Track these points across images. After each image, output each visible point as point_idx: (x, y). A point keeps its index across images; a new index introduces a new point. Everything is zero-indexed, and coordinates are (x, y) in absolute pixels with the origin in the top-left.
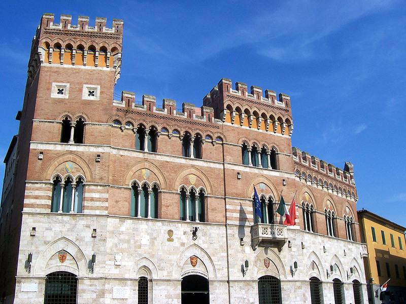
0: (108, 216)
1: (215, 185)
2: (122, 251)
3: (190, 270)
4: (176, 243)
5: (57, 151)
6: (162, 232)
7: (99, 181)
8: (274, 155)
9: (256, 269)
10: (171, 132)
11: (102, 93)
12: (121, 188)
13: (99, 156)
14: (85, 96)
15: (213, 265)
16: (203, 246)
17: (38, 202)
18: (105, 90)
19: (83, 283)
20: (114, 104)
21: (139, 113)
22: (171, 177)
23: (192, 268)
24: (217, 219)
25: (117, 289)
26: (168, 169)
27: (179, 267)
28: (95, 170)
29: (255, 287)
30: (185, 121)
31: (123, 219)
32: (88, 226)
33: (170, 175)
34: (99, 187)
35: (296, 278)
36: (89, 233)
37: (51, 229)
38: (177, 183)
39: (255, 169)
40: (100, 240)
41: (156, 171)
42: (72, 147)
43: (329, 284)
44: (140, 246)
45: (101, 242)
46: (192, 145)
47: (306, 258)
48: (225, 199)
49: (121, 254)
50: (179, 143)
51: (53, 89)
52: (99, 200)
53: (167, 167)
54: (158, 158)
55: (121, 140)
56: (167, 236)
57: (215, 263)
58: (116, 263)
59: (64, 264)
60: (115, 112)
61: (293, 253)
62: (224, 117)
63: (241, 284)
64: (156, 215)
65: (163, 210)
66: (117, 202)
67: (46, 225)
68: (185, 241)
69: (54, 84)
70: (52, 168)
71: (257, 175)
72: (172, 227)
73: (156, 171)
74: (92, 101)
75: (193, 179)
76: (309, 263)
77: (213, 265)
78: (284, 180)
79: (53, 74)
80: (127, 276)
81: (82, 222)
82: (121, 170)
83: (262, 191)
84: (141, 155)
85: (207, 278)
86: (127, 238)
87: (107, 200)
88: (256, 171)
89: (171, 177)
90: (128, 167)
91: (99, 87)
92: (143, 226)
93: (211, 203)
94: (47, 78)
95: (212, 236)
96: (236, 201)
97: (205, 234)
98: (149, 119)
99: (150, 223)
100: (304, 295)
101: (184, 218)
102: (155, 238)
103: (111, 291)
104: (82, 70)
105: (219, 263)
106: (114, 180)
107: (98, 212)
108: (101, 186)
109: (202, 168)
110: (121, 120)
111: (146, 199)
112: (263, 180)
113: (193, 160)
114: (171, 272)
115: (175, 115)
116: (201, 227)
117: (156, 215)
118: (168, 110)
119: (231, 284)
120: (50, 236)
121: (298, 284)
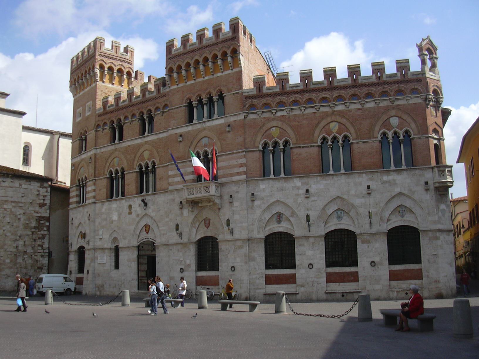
0: (95, 203)
4: (134, 215)
9: (194, 230)
16: (153, 214)
29: (192, 250)
31: (103, 203)
35: (236, 235)
38: (136, 162)
39: (191, 126)
43: (311, 240)
47: (258, 212)
50: (137, 124)
56: (128, 210)
61: (234, 209)
63: (179, 247)
64: (123, 195)
66: (100, 190)
68: (139, 212)
71: (200, 131)
75: (146, 154)
76: (268, 216)
80: (105, 246)
83: (205, 145)
84: (113, 147)
88: (199, 126)
92: (114, 205)
99: (118, 202)
101: (142, 192)
102: (121, 214)
105: (164, 228)
109: (152, 141)
113: (146, 136)
121: (239, 243)
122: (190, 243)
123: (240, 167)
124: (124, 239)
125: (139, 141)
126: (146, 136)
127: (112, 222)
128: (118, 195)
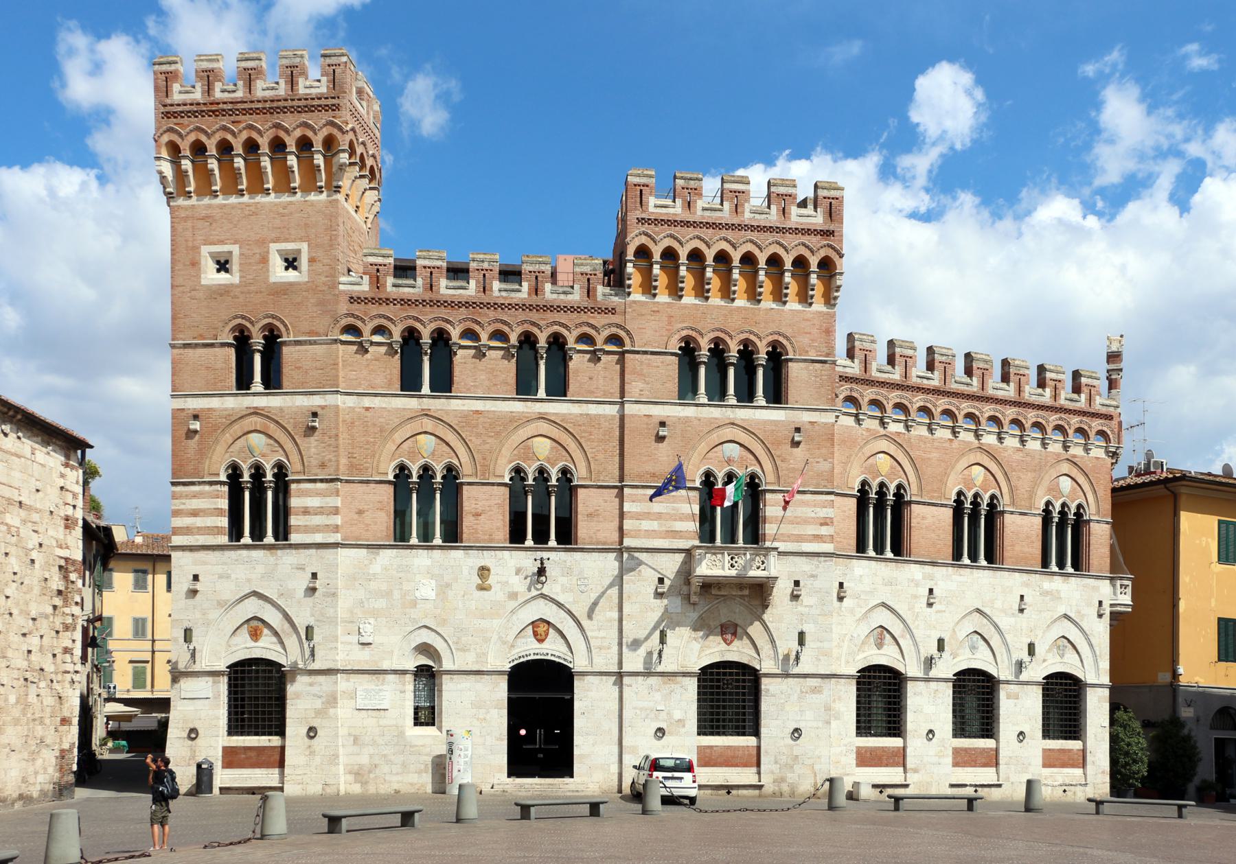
1: (601, 457)
2: (375, 614)
3: (531, 649)
4: (497, 594)
5: (226, 409)
6: (465, 572)
7: (318, 471)
8: (777, 358)
10: (484, 337)
11: (312, 260)
12: (368, 482)
13: (315, 415)
14: (278, 273)
15: (586, 638)
17: (199, 522)
18: (320, 254)
19: (293, 680)
20: (341, 287)
21: (405, 302)
22: (487, 446)
23: (537, 645)
24: (602, 536)
25: (366, 691)
26: (480, 429)
27: (505, 643)
28: (309, 448)
30: (523, 307)
32: (301, 568)
33: (484, 442)
34: (319, 485)
36: (304, 581)
37: (228, 577)
40: (326, 595)
41: (451, 437)
42: (259, 399)
44: (414, 603)
45: (329, 599)
46: (542, 363)
48: (621, 488)
49: (372, 621)
51: (203, 262)
52: (320, 511)
53: (476, 426)
54: (455, 405)
55: (365, 372)
57: (589, 634)
58: (363, 640)
59: (260, 644)
60: (344, 307)
62: (628, 282)
65: (468, 523)
67: (219, 569)
69: (205, 250)
70: (220, 449)
72: (487, 558)
73: (451, 437)
74: (291, 284)
75: (543, 447)
77: (586, 638)
78: (798, 430)
79: (200, 224)
81: (287, 558)
82: (368, 443)
84: (410, 403)
85: (571, 666)
86: (384, 587)
87: (336, 511)
89: (487, 446)
90: (385, 433)
91: (304, 247)
93: (586, 501)
94: (189, 234)
95: (578, 573)
96: (640, 491)
97: (568, 572)
98: (427, 314)
99: (437, 553)
100: (828, 709)
102: (448, 585)
103: (353, 695)
104: (263, 206)
105: (602, 634)
106: (352, 467)
107: (318, 538)
108: (322, 481)
110: (359, 324)
111: (426, 505)
112: (720, 433)
113: (541, 400)
114: (486, 655)
115: (496, 294)
116: (557, 559)
117: (453, 535)
118: (478, 282)
119: (626, 680)
120: (229, 591)
122: (685, 674)
123: (822, 524)
124: (464, 650)
125: (518, 407)
126: (541, 400)
127: (414, 603)
128: (426, 535)
